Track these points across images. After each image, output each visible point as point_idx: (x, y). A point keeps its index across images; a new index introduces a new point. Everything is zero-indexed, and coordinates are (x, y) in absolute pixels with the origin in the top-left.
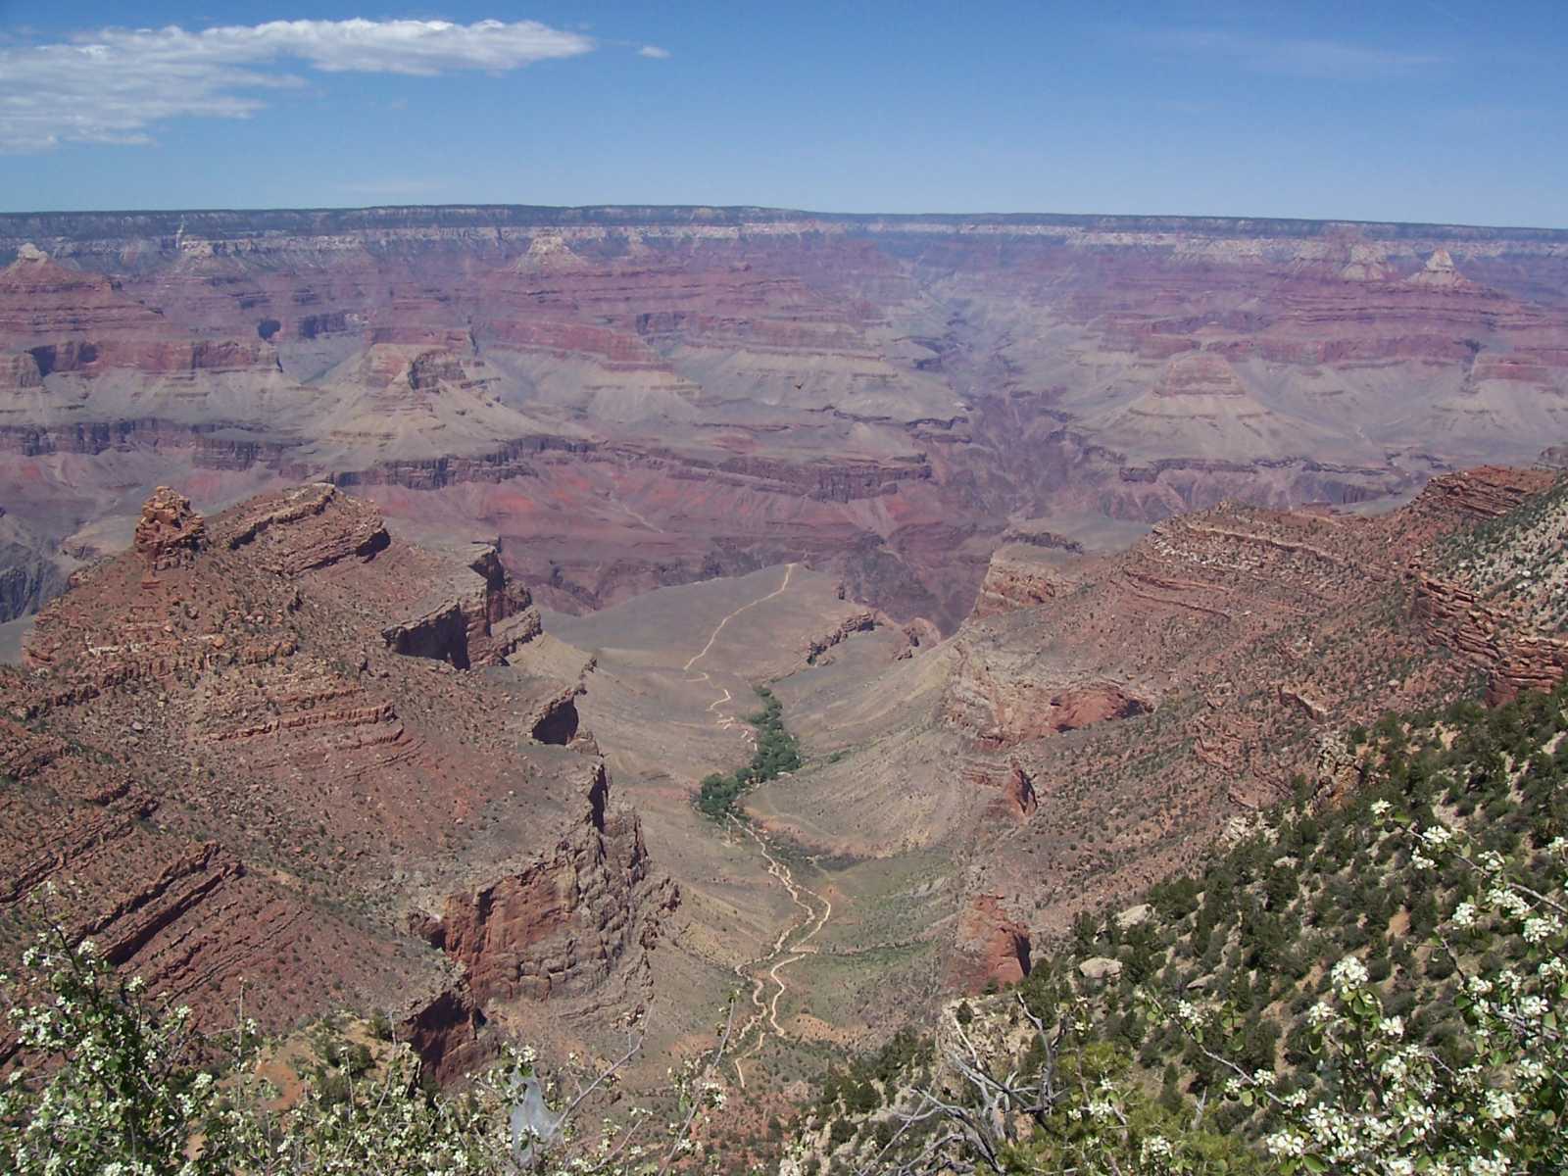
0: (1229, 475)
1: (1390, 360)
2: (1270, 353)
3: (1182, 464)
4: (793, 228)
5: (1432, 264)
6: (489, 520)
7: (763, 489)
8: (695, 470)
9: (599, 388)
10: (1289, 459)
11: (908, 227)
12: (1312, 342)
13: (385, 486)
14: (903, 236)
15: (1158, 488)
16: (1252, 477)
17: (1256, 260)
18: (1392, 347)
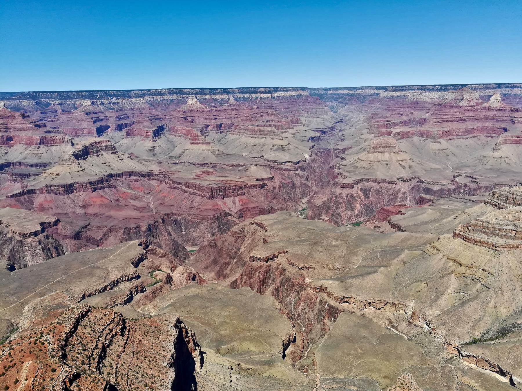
0: (386, 185)
1: (471, 135)
2: (422, 135)
3: (368, 180)
4: (293, 93)
5: (492, 99)
6: (84, 207)
7: (193, 194)
8: (176, 185)
9: (186, 150)
10: (412, 178)
11: (339, 92)
12: (436, 130)
13: (45, 194)
14: (338, 94)
15: (353, 191)
16: (394, 186)
17: (436, 100)
18: (470, 131)
